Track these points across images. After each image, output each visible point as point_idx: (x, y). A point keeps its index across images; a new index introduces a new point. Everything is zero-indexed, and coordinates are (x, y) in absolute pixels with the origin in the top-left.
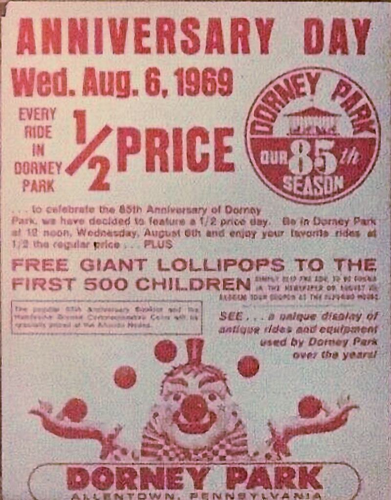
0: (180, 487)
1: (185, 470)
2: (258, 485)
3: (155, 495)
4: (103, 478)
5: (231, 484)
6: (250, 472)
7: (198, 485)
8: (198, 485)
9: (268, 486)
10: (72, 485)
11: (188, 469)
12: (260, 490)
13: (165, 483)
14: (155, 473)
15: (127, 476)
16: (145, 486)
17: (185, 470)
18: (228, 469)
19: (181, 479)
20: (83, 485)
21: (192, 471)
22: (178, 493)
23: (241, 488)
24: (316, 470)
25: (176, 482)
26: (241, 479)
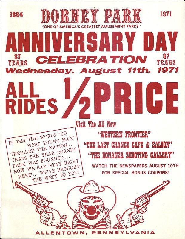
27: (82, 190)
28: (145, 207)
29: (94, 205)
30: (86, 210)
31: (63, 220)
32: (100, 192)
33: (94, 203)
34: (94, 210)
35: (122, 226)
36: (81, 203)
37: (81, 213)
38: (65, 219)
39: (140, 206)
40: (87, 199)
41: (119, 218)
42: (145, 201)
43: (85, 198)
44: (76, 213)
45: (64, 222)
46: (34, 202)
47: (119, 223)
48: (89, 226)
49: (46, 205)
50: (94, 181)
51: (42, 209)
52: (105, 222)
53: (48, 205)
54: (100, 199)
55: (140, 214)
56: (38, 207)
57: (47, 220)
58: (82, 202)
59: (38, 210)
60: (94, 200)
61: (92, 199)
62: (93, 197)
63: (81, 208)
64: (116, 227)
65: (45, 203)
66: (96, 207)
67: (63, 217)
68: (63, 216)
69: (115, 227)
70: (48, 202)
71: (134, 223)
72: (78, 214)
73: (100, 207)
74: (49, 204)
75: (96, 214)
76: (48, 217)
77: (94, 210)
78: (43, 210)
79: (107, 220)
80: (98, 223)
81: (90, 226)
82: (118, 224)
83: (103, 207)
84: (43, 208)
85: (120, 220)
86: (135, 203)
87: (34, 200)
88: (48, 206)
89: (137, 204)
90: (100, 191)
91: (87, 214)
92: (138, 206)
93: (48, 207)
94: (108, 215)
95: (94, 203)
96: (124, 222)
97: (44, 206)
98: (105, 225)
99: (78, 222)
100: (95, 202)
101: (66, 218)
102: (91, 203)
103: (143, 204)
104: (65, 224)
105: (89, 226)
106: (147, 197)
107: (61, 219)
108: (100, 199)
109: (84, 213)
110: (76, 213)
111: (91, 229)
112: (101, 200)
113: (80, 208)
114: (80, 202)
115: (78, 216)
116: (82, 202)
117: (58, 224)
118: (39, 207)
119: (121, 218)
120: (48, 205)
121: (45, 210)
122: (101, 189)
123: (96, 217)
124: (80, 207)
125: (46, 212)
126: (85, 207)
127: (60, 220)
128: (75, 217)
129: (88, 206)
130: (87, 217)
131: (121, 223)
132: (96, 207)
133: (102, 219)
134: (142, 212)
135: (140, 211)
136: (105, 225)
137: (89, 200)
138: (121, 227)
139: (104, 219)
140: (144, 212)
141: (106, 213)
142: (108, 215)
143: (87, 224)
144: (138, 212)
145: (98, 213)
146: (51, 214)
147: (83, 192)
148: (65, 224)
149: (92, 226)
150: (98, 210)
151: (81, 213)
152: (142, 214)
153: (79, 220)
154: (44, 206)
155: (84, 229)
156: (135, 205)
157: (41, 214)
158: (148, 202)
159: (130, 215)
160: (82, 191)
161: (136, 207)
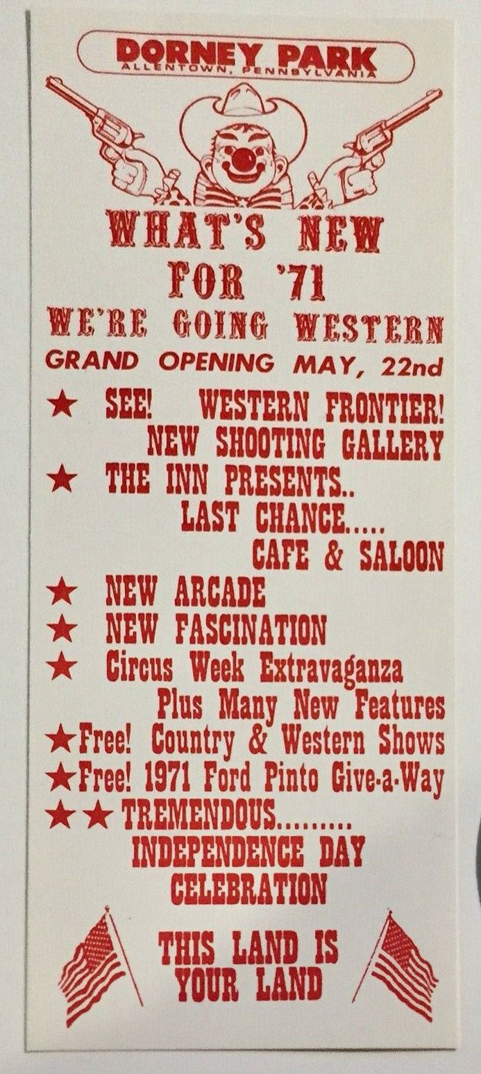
0: (232, 62)
1: (237, 47)
2: (312, 63)
3: (207, 67)
4: (153, 51)
5: (283, 61)
6: (302, 50)
7: (250, 61)
8: (250, 61)
9: (319, 64)
10: (122, 56)
11: (240, 45)
12: (312, 68)
13: (217, 59)
14: (206, 48)
15: (177, 49)
16: (195, 60)
17: (236, 45)
18: (280, 46)
19: (232, 54)
20: (132, 57)
21: (244, 47)
22: (229, 68)
23: (293, 65)
24: (370, 51)
25: (228, 57)
26: (294, 57)
27: (219, 106)
28: (379, 154)
29: (252, 146)
30: (229, 158)
31: (170, 182)
32: (264, 112)
33: (249, 141)
34: (250, 158)
35: (321, 201)
36: (217, 142)
37: (218, 167)
38: (176, 180)
39: (367, 151)
40: (231, 131)
41: (313, 181)
42: (380, 139)
43: (228, 128)
44: (203, 166)
45: (174, 188)
46: (97, 135)
47: (315, 195)
48: (236, 199)
49: (128, 142)
50: (249, 85)
51: (117, 152)
52: (278, 190)
53: (132, 142)
54: (266, 133)
55: (367, 174)
56: (106, 147)
57: (130, 180)
58: (218, 138)
59: (105, 153)
60: (250, 133)
61: (245, 131)
62: (247, 127)
63: (217, 155)
64: (306, 203)
65: (124, 136)
66: (254, 151)
67: (171, 175)
68: (171, 172)
69: (304, 204)
70: (133, 134)
71: (350, 195)
72: (210, 168)
73: (265, 152)
74: (134, 139)
75: (254, 171)
76: (134, 173)
77: (250, 158)
78: (120, 155)
79: (284, 186)
80: (261, 192)
81: (240, 198)
82: (312, 198)
83: (274, 153)
84: (120, 150)
85: (317, 186)
86: (355, 144)
87: (96, 126)
88: (131, 144)
89: (359, 147)
90: (266, 111)
91: (233, 169)
92: (362, 152)
93: (131, 148)
94: (286, 174)
95: (249, 141)
96: (326, 193)
97: (123, 145)
98: (279, 199)
99: (208, 189)
100: (252, 138)
101: (178, 177)
102: (242, 141)
103: (375, 148)
104: (177, 192)
105: (236, 199)
106: (387, 130)
107: (166, 180)
108: (264, 132)
109: (226, 166)
110: (203, 166)
111: (242, 206)
112: (269, 134)
113: (214, 154)
114: (215, 138)
115: (209, 173)
116: (218, 138)
117: (158, 191)
118: (109, 146)
119: (319, 183)
120: (132, 142)
121: (123, 156)
122: (269, 107)
123: (257, 176)
124: (214, 150)
125: (127, 159)
126: (228, 150)
127: (163, 182)
128: (201, 175)
129: (234, 150)
130: (231, 176)
131: (320, 193)
132: (254, 151)
133: (272, 183)
134: (373, 169)
135: (368, 165)
136: (279, 199)
137: (238, 133)
138: (318, 203)
139: (278, 182)
140: (377, 168)
141: (280, 167)
142: (286, 174)
143: (233, 196)
144: (363, 167)
145: (261, 167)
146: (139, 166)
147: (222, 113)
148: (177, 192)
149: (246, 199)
150: (259, 159)
151: (218, 167)
152: (372, 172)
153: (212, 183)
154: (123, 145)
155: (223, 206)
156: (355, 147)
157: (114, 165)
158: (388, 142)
159: (342, 174)
160: (220, 109)
161: (356, 154)
